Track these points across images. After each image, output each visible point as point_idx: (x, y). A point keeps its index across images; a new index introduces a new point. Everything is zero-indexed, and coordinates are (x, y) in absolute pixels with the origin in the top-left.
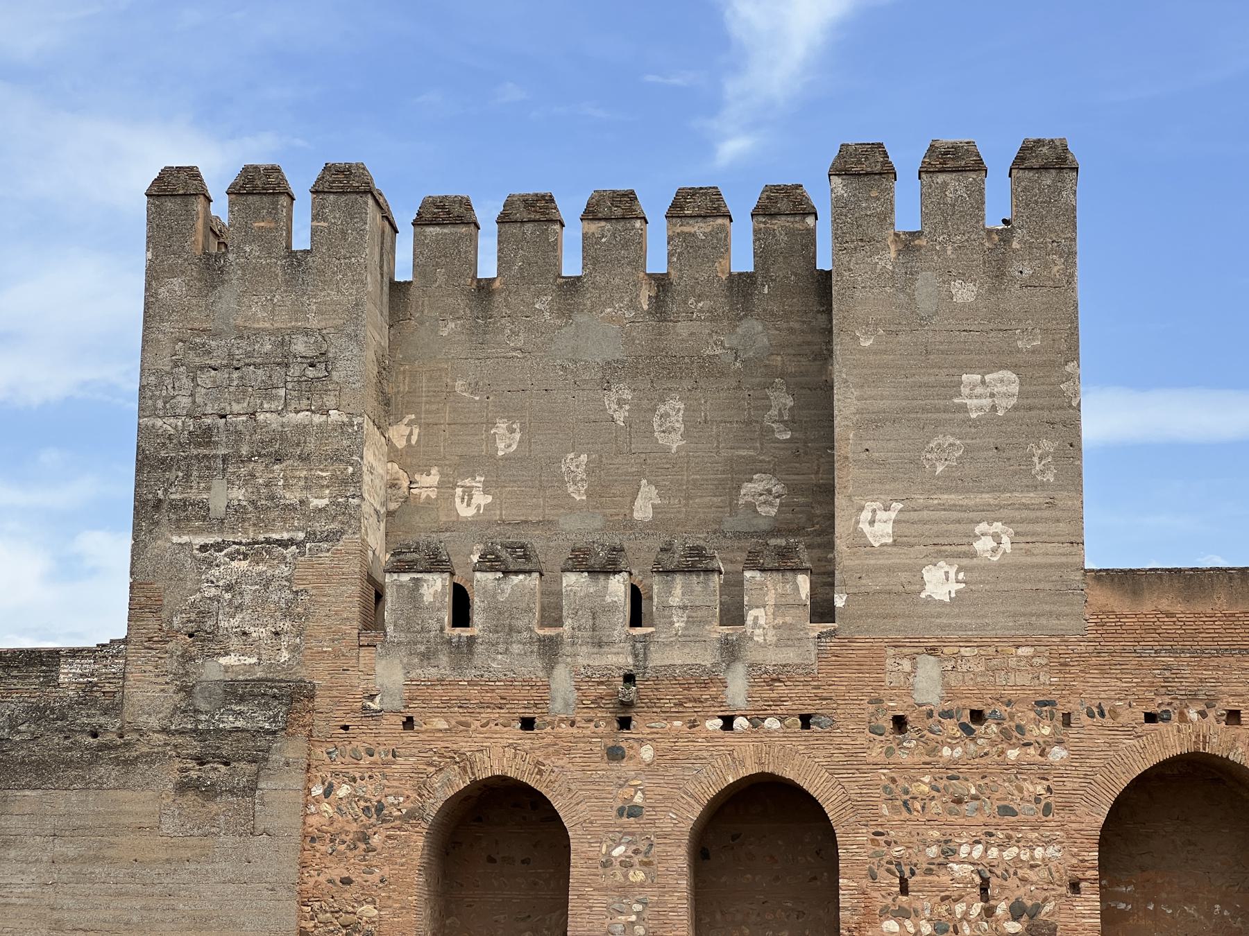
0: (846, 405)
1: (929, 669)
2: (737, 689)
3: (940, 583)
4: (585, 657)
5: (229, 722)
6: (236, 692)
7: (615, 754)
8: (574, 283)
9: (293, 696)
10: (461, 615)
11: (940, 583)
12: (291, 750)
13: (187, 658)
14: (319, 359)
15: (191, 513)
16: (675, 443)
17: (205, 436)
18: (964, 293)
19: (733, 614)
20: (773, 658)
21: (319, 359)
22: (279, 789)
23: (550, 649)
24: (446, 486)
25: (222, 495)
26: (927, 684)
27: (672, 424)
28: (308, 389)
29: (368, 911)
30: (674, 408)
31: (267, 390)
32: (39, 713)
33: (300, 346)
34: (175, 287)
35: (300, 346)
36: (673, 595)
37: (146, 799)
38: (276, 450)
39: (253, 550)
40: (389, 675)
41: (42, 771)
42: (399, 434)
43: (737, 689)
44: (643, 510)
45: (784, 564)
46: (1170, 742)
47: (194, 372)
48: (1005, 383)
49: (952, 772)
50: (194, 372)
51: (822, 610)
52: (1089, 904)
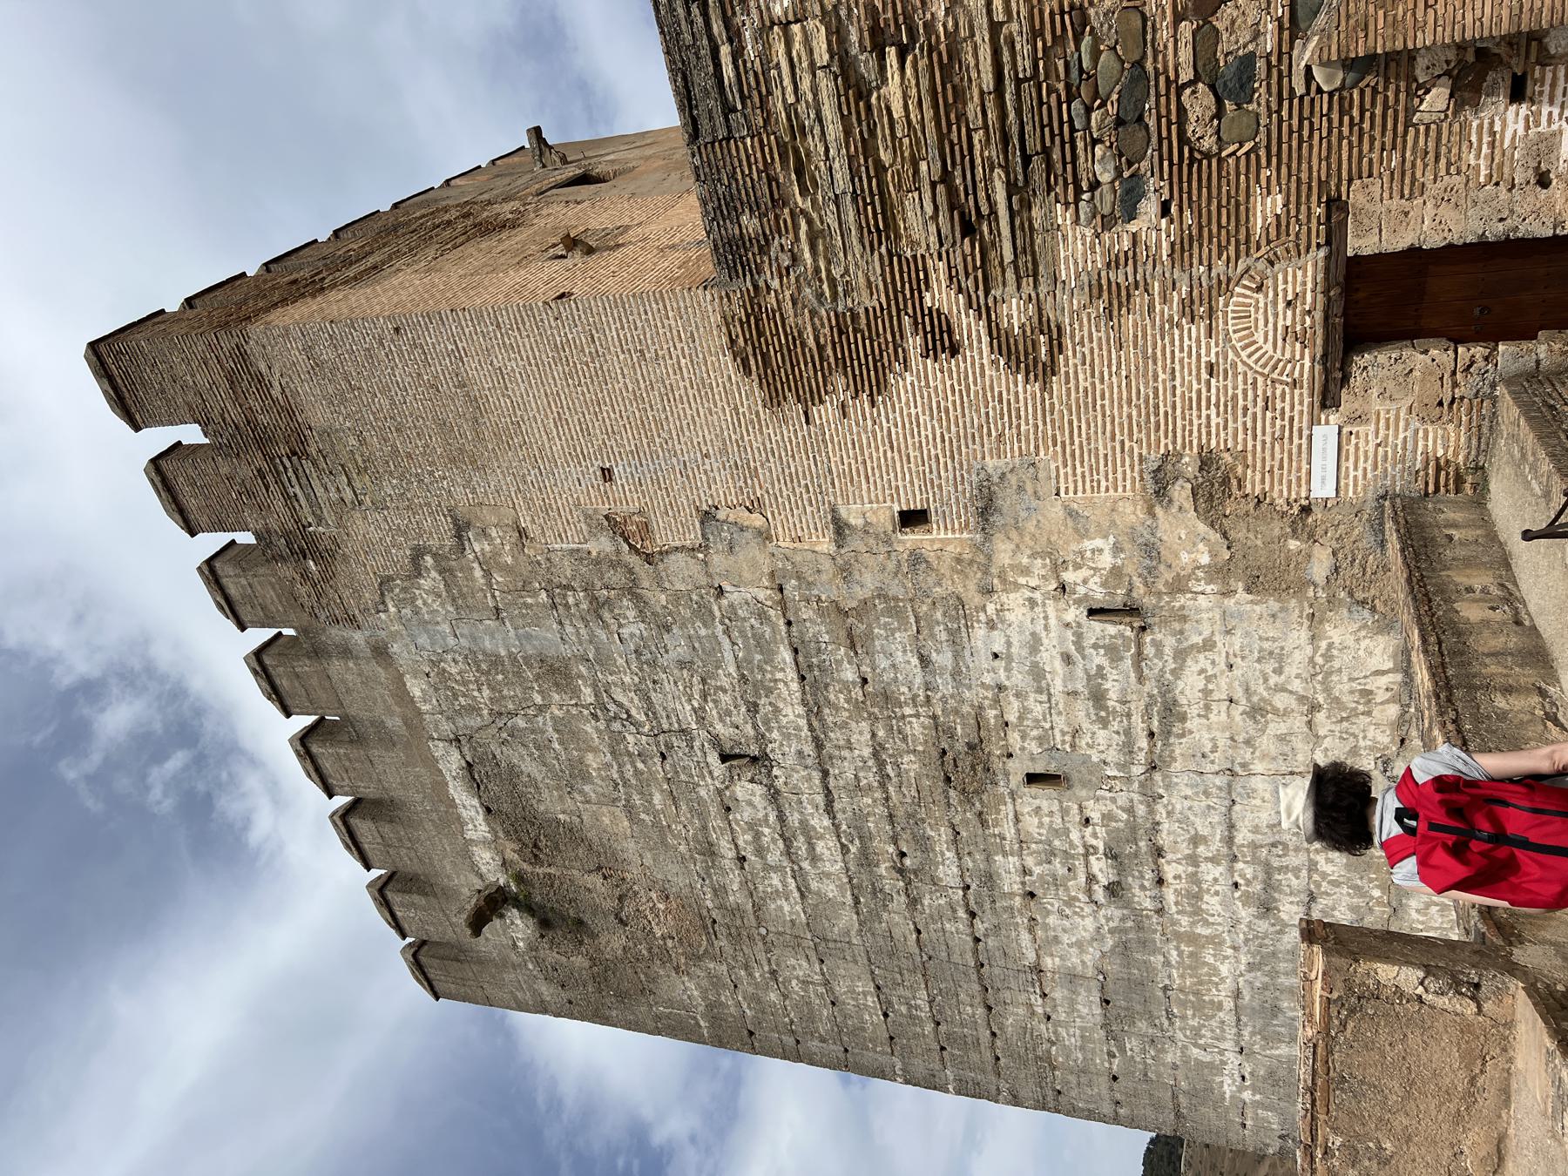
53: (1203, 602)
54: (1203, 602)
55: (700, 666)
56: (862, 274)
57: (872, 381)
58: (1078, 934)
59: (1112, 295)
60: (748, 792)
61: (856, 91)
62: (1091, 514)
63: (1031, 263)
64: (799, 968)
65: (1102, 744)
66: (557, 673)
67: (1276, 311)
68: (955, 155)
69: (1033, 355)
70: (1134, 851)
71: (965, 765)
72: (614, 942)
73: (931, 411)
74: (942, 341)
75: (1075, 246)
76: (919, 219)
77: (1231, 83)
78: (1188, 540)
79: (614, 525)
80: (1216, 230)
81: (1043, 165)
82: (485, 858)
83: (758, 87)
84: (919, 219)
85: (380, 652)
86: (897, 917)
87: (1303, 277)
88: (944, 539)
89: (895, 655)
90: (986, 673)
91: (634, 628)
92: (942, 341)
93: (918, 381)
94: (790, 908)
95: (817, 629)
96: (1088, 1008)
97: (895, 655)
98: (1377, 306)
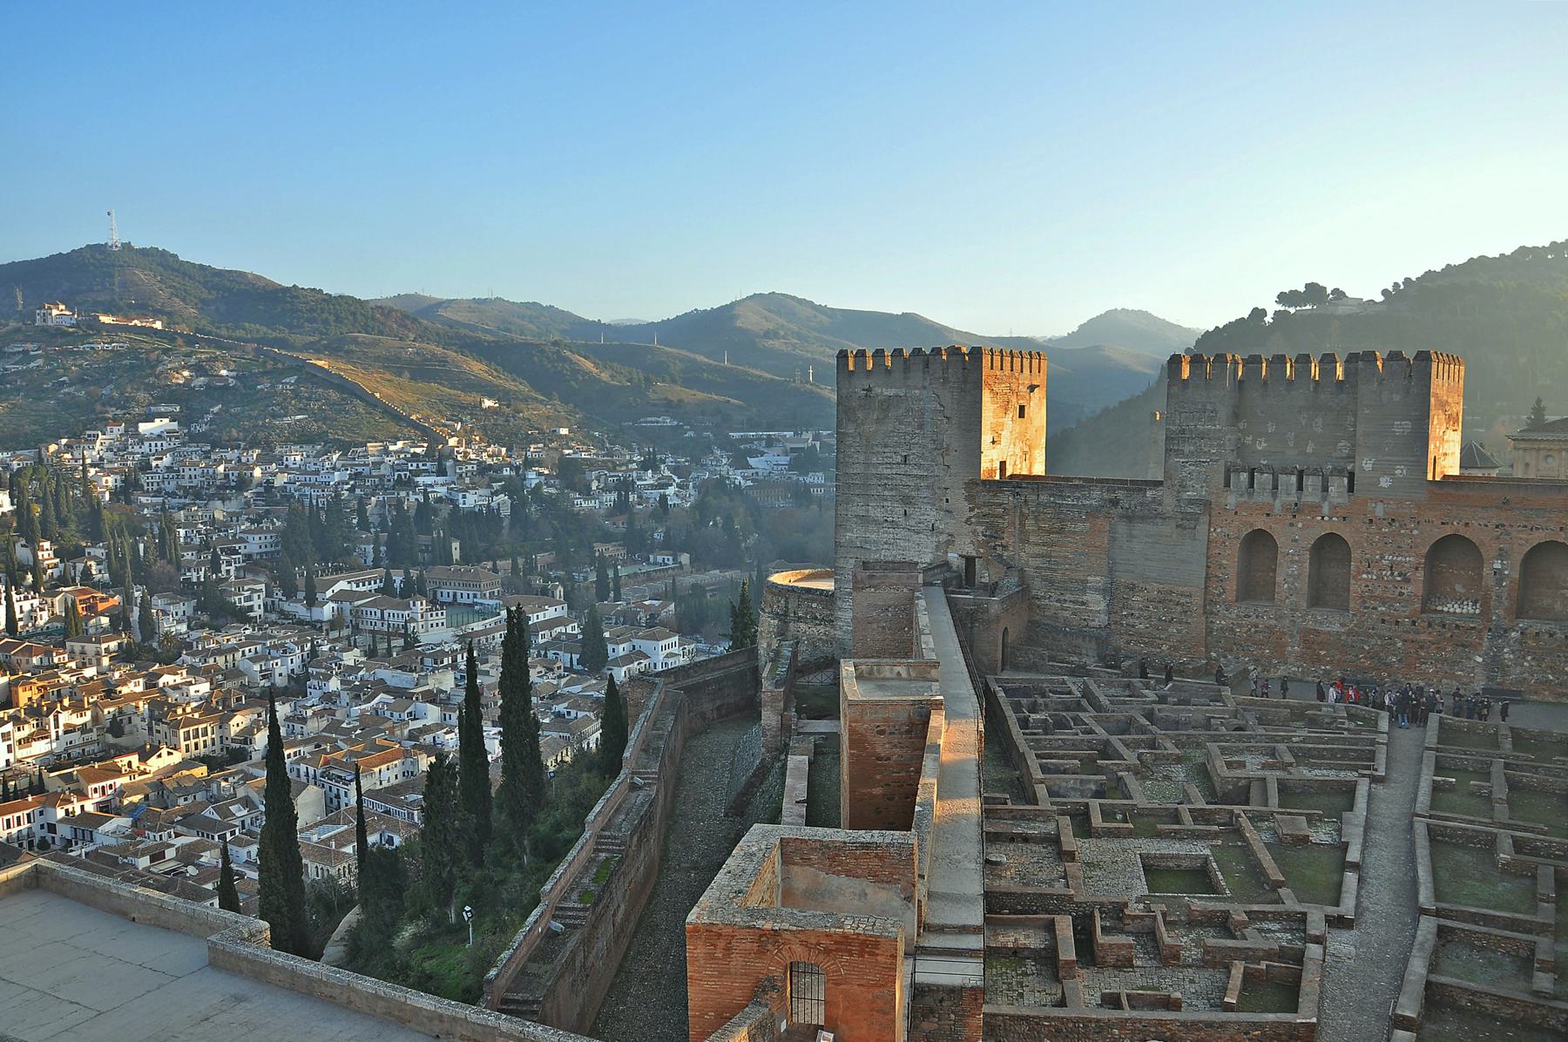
0: (1360, 429)
1: (1380, 506)
2: (1326, 510)
3: (1385, 482)
4: (1284, 498)
6: (1191, 502)
7: (1291, 525)
8: (1290, 382)
9: (1206, 504)
10: (1251, 485)
11: (1385, 482)
15: (1179, 453)
16: (1320, 430)
17: (1183, 432)
18: (1397, 398)
19: (1325, 489)
20: (1336, 501)
22: (1202, 529)
23: (1275, 496)
24: (1254, 440)
25: (1187, 448)
26: (1379, 510)
27: (1318, 426)
28: (1211, 419)
30: (1319, 421)
31: (1199, 419)
32: (1141, 504)
34: (1175, 389)
36: (1309, 481)
37: (1168, 528)
38: (1202, 436)
39: (1196, 464)
40: (1231, 500)
41: (1143, 519)
42: (1241, 425)
43: (1326, 510)
44: (1309, 450)
45: (1339, 472)
46: (1448, 531)
48: (1407, 425)
49: (1384, 535)
51: (1351, 489)
52: (1420, 574)
55: (922, 456)
56: (980, 500)
58: (878, 514)
60: (899, 459)
63: (979, 523)
64: (862, 458)
65: (912, 522)
66: (921, 426)
67: (970, 551)
69: (968, 521)
71: (907, 500)
74: (971, 510)
75: (980, 529)
76: (985, 510)
78: (943, 538)
80: (980, 545)
81: (990, 526)
84: (985, 510)
86: (875, 481)
92: (971, 510)
93: (966, 505)
94: (874, 460)
95: (931, 480)
98: (970, 561)
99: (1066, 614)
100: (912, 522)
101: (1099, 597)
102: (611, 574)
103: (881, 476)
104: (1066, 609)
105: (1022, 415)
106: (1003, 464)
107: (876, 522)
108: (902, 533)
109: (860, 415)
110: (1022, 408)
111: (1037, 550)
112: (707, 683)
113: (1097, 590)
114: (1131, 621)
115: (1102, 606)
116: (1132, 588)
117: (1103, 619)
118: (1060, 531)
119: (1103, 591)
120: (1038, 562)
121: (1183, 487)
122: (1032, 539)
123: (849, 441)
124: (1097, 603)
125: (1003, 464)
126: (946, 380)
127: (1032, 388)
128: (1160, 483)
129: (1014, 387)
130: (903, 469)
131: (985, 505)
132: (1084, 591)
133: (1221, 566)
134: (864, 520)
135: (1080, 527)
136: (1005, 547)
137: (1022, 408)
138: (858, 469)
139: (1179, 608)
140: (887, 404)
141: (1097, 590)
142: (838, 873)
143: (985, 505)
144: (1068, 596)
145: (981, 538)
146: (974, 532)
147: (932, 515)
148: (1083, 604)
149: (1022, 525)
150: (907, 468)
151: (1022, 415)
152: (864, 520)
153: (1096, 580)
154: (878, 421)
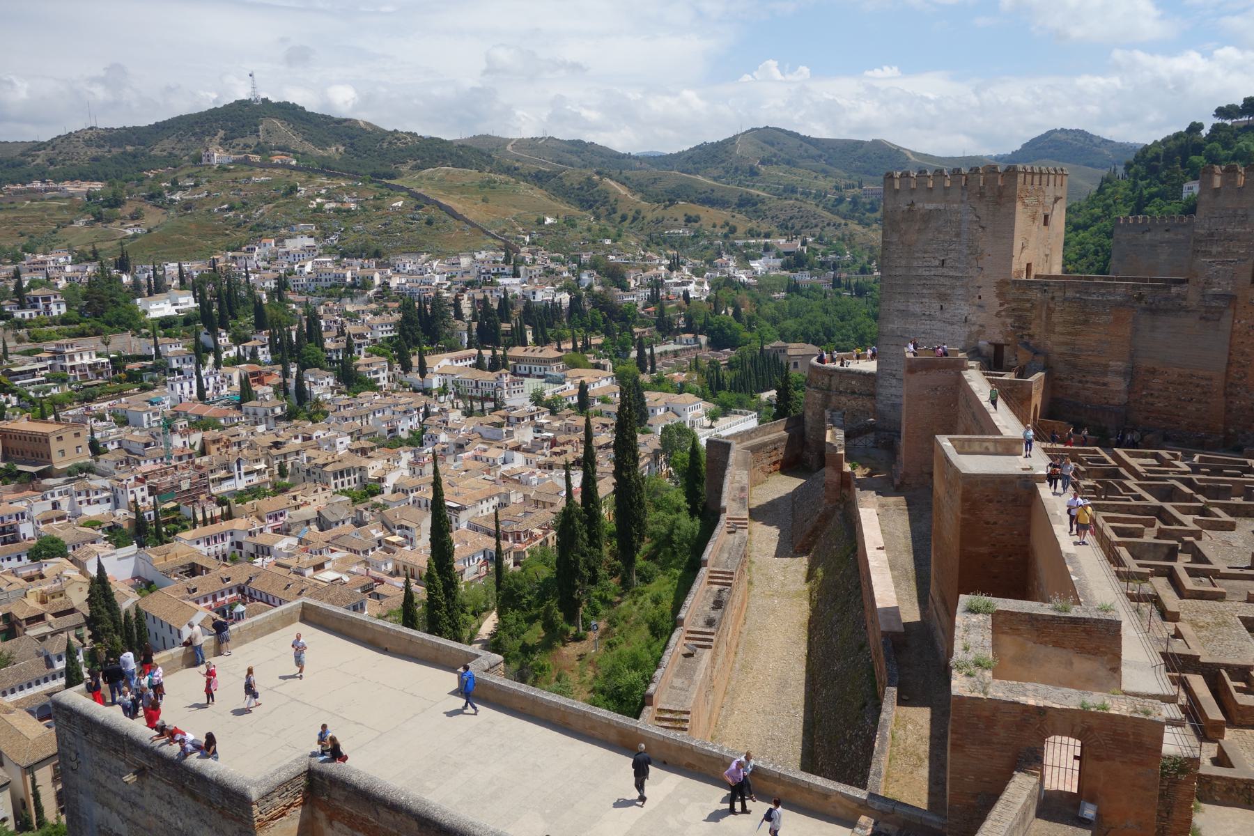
5: (1214, 304)
6: (1216, 297)
12: (1231, 311)
13: (1204, 288)
14: (1246, 215)
15: (1207, 254)
17: (1212, 235)
21: (1246, 215)
29: (1247, 350)
32: (1166, 299)
33: (1240, 212)
35: (1240, 212)
38: (1231, 238)
39: (1223, 263)
47: (1210, 219)
50: (1210, 219)
53: (967, 329)
54: (967, 329)
57: (998, 296)
59: (1004, 324)
60: (937, 263)
61: (1028, 301)
62: (978, 318)
63: (1008, 316)
64: (904, 263)
65: (947, 316)
66: (958, 235)
67: (999, 339)
68: (1020, 310)
69: (998, 314)
70: (931, 317)
71: (943, 297)
72: (903, 226)
73: (993, 301)
74: (1001, 305)
75: (1009, 321)
77: (1022, 337)
78: (975, 328)
79: (981, 253)
81: (1019, 318)
82: (920, 205)
83: (1031, 289)
84: (1014, 305)
85: (962, 202)
86: (915, 282)
87: (1003, 342)
88: (977, 301)
89: (960, 291)
90: (958, 303)
91: (966, 252)
93: (997, 301)
94: (915, 264)
95: (966, 280)
96: (902, 308)
97: (960, 291)
99: (1087, 393)
100: (947, 316)
101: (1120, 379)
102: (648, 351)
103: (920, 277)
104: (1087, 389)
105: (1046, 223)
106: (1029, 265)
107: (914, 314)
108: (939, 325)
109: (903, 226)
110: (1046, 217)
111: (1062, 339)
112: (764, 445)
113: (1117, 373)
114: (1150, 400)
115: (1123, 386)
116: (1153, 372)
117: (1123, 398)
118: (1086, 322)
119: (1125, 374)
120: (1063, 349)
121: (1208, 283)
122: (1057, 329)
123: (893, 248)
124: (1118, 385)
125: (1029, 265)
126: (982, 195)
127: (1057, 199)
128: (1186, 281)
129: (1041, 199)
130: (940, 271)
131: (1014, 300)
132: (1105, 374)
133: (1243, 353)
134: (905, 314)
135: (1104, 319)
136: (1031, 336)
137: (1046, 217)
138: (900, 272)
139: (1199, 390)
140: (928, 217)
141: (1117, 373)
142: (1045, 643)
143: (1014, 300)
144: (1090, 378)
145: (1009, 328)
146: (1004, 324)
147: (964, 309)
148: (1104, 384)
149: (1049, 317)
150: (945, 271)
151: (1046, 223)
152: (905, 314)
153: (1118, 365)
154: (919, 231)
